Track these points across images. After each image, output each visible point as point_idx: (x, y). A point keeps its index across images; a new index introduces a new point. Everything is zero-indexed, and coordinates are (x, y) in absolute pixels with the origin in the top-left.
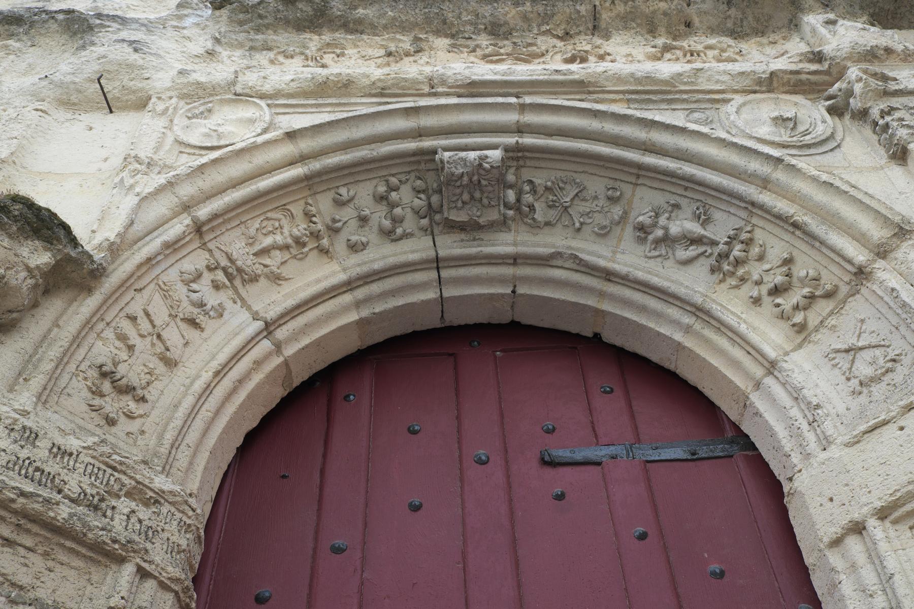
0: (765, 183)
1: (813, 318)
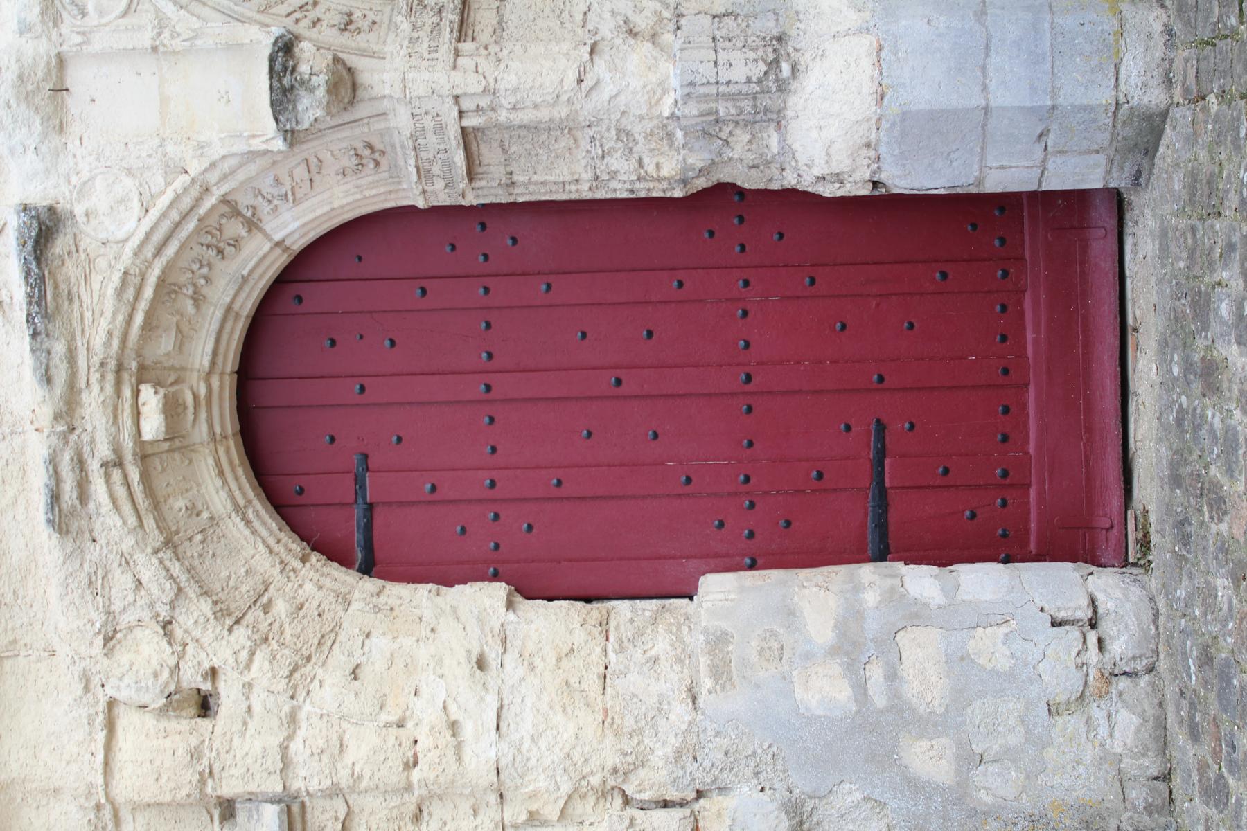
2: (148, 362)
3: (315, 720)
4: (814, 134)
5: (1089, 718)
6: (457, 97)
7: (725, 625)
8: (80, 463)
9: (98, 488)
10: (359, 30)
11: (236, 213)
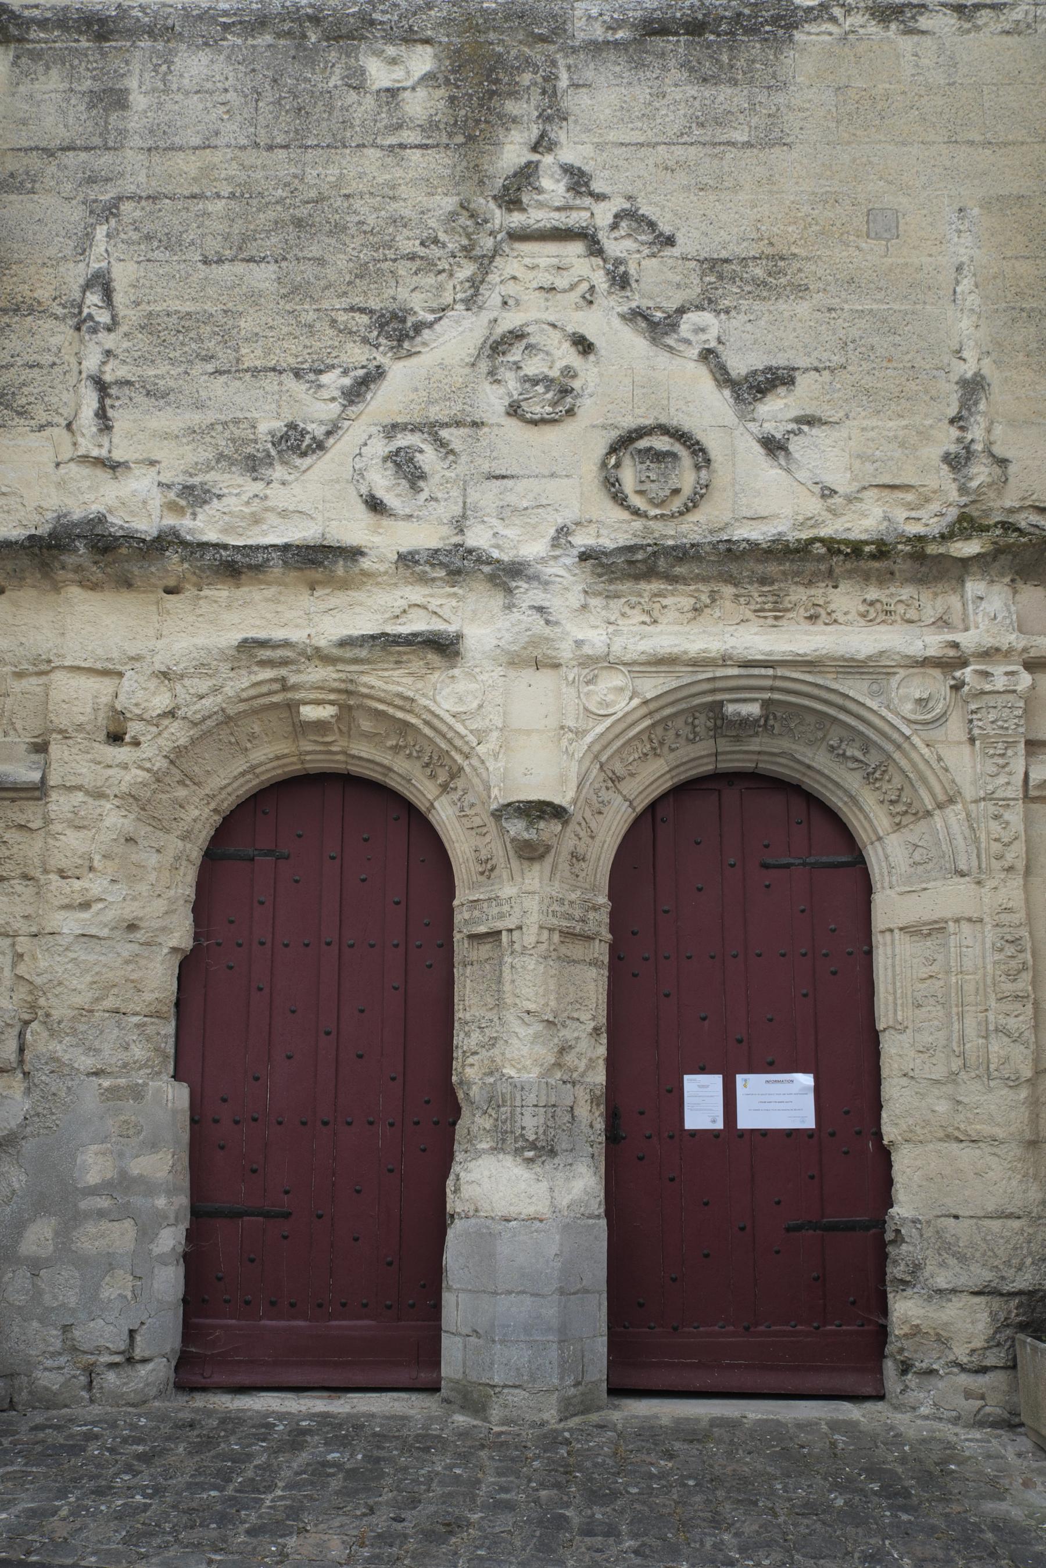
0: (899, 747)
1: (908, 819)
2: (355, 713)
3: (99, 811)
4: (486, 1173)
5: (60, 1354)
6: (520, 928)
8: (285, 663)
9: (268, 674)
10: (572, 865)
11: (453, 776)
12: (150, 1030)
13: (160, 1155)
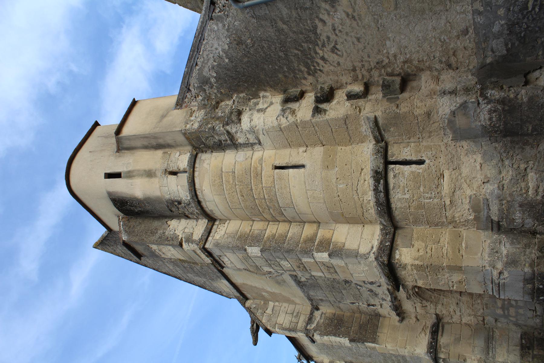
7: (487, 303)
12: (475, 299)
13: (498, 302)
